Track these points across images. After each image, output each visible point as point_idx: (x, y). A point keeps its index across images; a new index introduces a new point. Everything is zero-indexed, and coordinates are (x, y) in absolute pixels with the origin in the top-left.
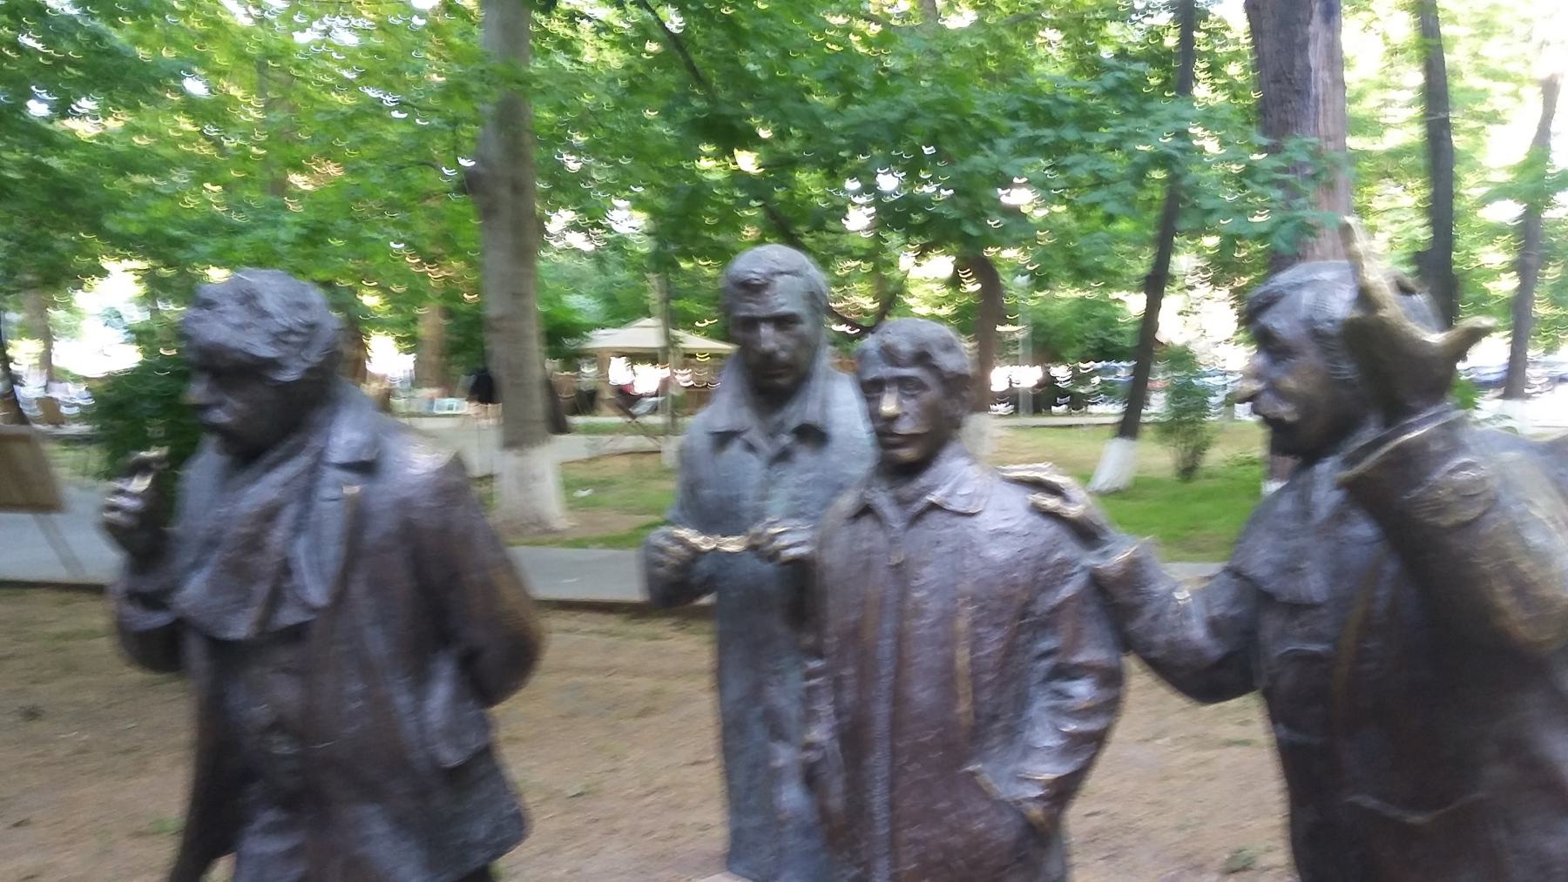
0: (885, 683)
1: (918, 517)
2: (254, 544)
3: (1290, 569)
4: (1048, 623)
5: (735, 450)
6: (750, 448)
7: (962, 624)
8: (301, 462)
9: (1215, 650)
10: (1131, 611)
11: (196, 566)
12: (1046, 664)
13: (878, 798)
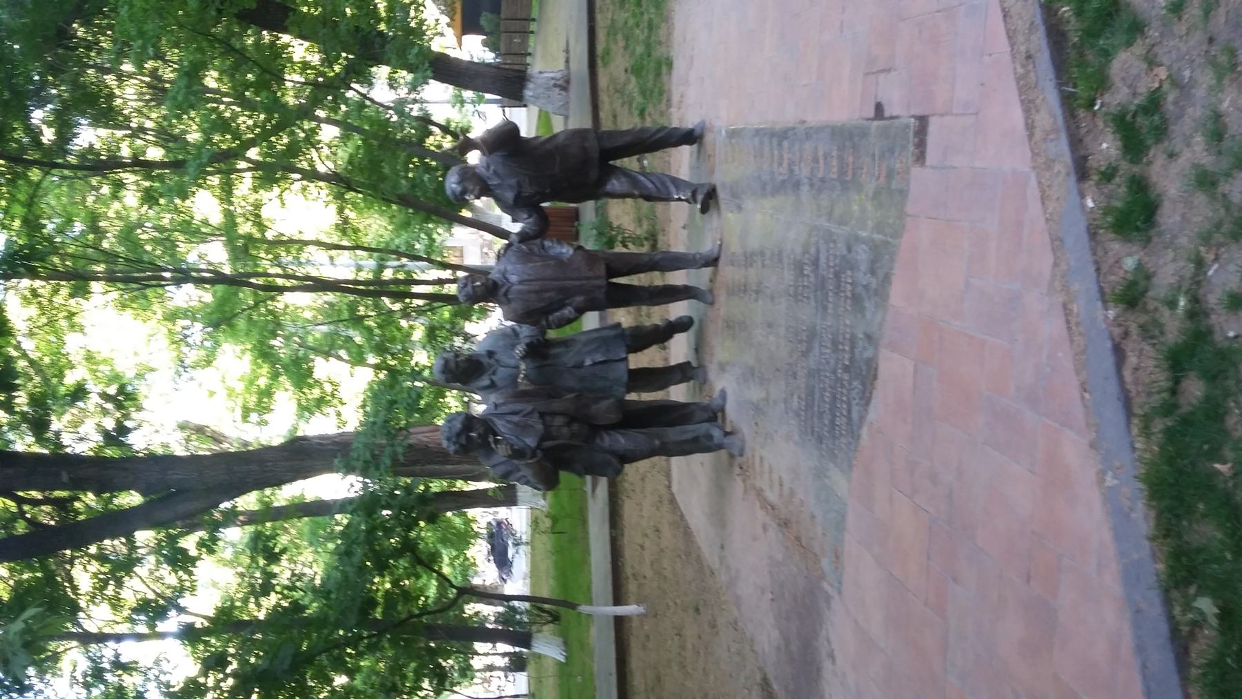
0: (547, 282)
1: (507, 279)
2: (516, 424)
3: (511, 187)
4: (531, 252)
5: (494, 378)
6: (494, 373)
7: (531, 265)
8: (495, 419)
9: (535, 216)
10: (527, 233)
11: (524, 442)
12: (542, 250)
13: (577, 283)
